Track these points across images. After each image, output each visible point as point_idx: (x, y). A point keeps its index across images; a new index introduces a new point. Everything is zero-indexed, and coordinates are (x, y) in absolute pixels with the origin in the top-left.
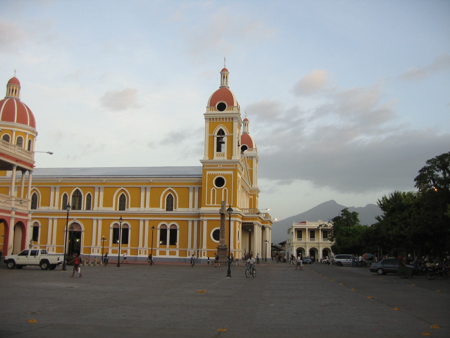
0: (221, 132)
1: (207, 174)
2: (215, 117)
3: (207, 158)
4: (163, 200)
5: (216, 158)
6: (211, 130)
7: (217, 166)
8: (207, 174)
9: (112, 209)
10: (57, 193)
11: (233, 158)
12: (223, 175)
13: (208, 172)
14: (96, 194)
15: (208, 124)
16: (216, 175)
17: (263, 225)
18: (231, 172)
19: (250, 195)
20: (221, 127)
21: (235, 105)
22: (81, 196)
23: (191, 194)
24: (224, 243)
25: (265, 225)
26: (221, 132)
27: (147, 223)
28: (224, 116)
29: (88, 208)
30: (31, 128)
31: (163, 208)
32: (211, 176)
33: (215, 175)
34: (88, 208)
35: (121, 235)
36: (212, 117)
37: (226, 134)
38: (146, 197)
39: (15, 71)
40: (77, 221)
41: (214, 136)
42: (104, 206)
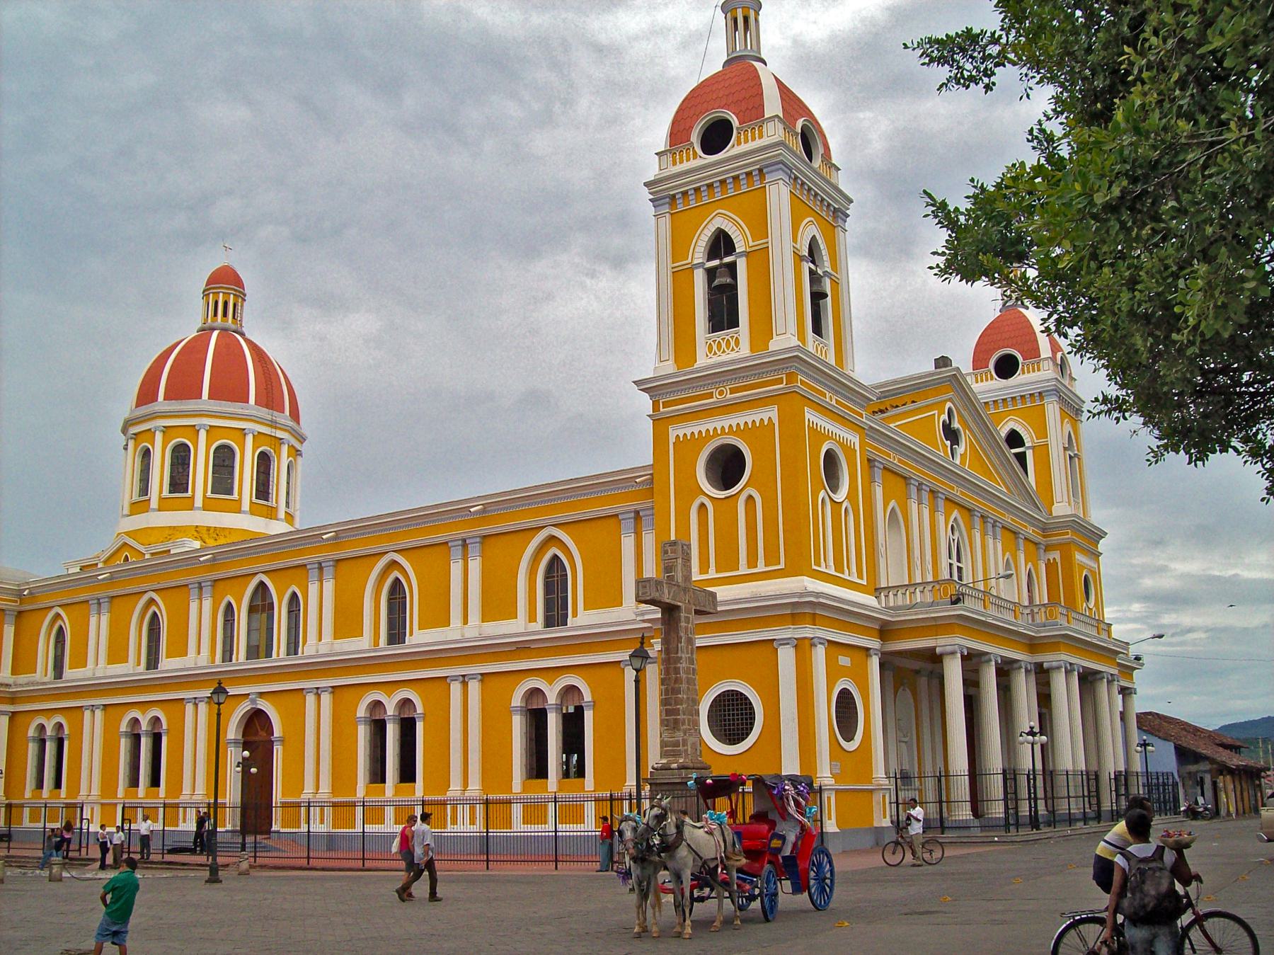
0: (721, 244)
1: (672, 439)
2: (688, 183)
3: (669, 367)
4: (528, 588)
5: (703, 360)
6: (679, 246)
7: (711, 395)
8: (672, 439)
9: (360, 645)
10: (207, 604)
11: (774, 345)
12: (738, 431)
13: (675, 432)
14: (313, 589)
15: (666, 222)
16: (709, 436)
17: (1038, 658)
18: (770, 414)
19: (1048, 548)
20: (719, 223)
21: (773, 106)
22: (271, 606)
23: (628, 543)
24: (676, 754)
25: (1048, 659)
26: (721, 244)
27: (474, 686)
28: (727, 171)
29: (293, 647)
30: (264, 413)
31: (532, 618)
32: (688, 446)
33: (703, 439)
34: (293, 647)
35: (398, 745)
36: (675, 188)
37: (740, 247)
38: (466, 575)
40: (263, 705)
41: (693, 267)
42: (338, 634)
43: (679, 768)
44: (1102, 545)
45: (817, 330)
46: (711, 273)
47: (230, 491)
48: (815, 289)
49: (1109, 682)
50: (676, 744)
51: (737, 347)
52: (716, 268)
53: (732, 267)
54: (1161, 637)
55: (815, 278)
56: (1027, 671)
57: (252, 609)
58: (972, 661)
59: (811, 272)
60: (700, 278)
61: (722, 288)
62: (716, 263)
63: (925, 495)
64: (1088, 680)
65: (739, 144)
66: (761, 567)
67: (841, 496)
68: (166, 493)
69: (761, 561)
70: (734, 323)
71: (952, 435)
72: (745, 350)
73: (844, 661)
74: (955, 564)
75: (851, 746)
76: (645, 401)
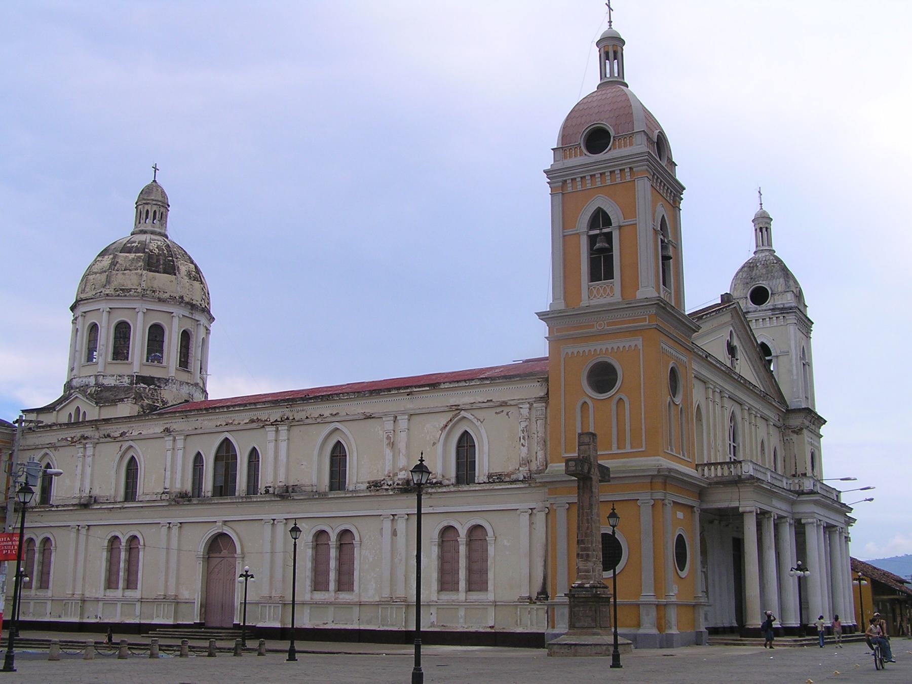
0: (600, 218)
24: (587, 578)
26: (600, 218)
39: (156, 169)
40: (227, 530)
43: (591, 587)
44: (823, 430)
45: (664, 284)
46: (592, 240)
47: (159, 360)
48: (665, 254)
49: (840, 533)
50: (588, 571)
51: (611, 293)
52: (596, 235)
53: (609, 237)
54: (871, 500)
55: (664, 247)
56: (790, 524)
57: (217, 458)
58: (762, 516)
59: (662, 241)
60: (584, 242)
61: (601, 250)
62: (597, 232)
63: (717, 395)
64: (829, 529)
65: (615, 148)
66: (628, 449)
67: (678, 400)
68: (110, 359)
69: (628, 446)
70: (609, 275)
71: (732, 350)
72: (617, 297)
73: (680, 515)
74: (732, 444)
75: (683, 574)
76: (543, 328)
